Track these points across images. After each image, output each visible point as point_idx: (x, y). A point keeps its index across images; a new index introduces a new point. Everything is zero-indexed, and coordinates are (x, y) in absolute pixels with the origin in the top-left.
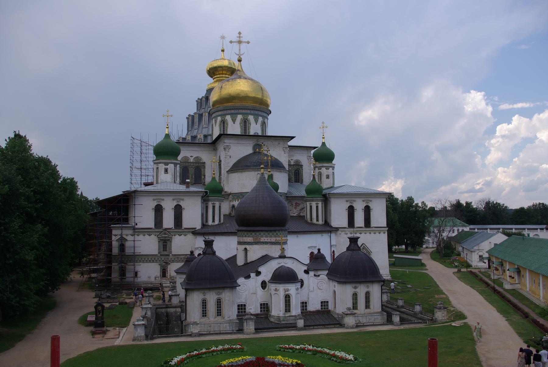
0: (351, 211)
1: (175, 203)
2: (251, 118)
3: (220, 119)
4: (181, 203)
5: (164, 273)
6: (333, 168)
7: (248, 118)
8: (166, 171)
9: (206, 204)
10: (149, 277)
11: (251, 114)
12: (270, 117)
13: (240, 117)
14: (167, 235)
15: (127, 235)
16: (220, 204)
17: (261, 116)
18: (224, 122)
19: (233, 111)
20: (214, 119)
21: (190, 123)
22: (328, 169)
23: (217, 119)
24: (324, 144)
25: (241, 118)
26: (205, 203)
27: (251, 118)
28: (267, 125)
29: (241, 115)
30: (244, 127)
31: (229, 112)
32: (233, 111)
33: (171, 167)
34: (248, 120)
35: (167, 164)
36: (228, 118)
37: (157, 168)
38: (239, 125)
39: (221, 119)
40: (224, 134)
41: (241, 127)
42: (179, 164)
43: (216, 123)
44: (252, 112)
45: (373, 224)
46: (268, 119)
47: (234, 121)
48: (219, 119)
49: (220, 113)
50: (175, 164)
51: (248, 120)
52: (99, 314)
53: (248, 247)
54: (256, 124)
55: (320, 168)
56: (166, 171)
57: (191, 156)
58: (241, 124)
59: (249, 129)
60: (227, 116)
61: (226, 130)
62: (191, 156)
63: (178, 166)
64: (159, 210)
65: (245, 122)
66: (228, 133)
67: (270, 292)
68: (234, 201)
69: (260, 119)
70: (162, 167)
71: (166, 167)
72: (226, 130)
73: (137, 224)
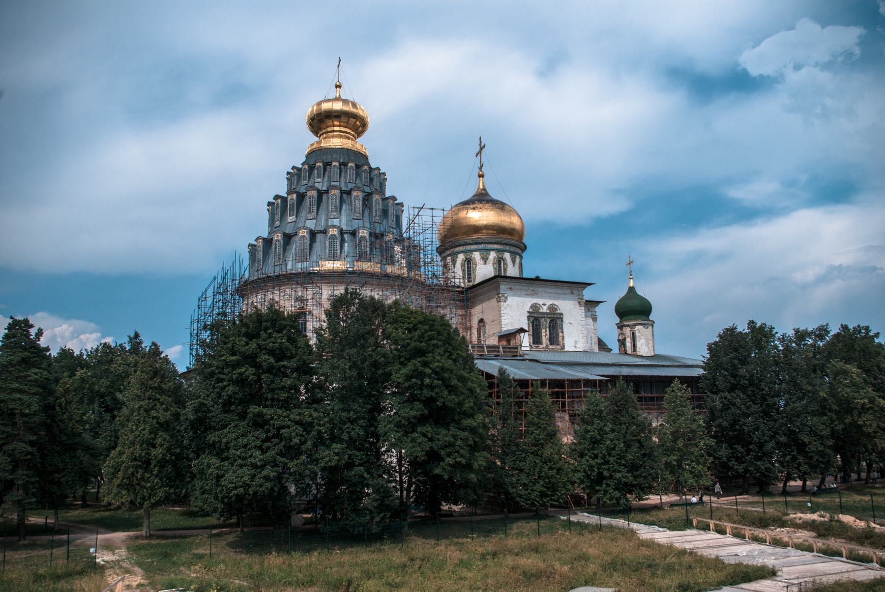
2: (507, 256)
11: (507, 251)
13: (493, 255)
20: (449, 259)
23: (457, 257)
34: (503, 260)
36: (477, 256)
40: (500, 276)
49: (461, 248)
51: (503, 260)
54: (514, 266)
60: (474, 253)
61: (473, 273)
65: (499, 262)
72: (473, 273)
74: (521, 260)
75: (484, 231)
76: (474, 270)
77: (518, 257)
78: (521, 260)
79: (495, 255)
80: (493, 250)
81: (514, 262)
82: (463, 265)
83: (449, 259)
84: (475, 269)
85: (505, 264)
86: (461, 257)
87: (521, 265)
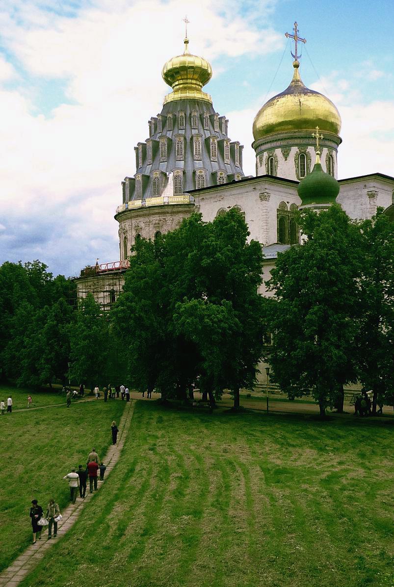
3: (267, 155)
7: (308, 150)
12: (340, 148)
13: (294, 150)
18: (272, 159)
21: (140, 155)
28: (335, 159)
30: (301, 165)
31: (278, 143)
34: (306, 155)
36: (278, 152)
38: (294, 162)
39: (269, 155)
40: (272, 177)
41: (297, 164)
46: (337, 152)
47: (286, 155)
65: (302, 157)
66: (278, 176)
75: (277, 129)
76: (275, 167)
79: (298, 150)
84: (276, 167)
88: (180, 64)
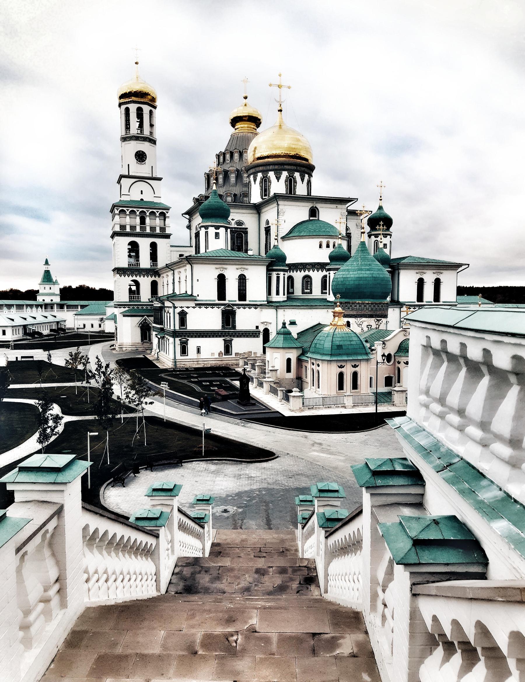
0: (421, 283)
1: (239, 272)
2: (297, 175)
4: (245, 273)
5: (228, 349)
6: (391, 235)
7: (295, 175)
8: (217, 235)
9: (269, 274)
10: (213, 354)
13: (285, 174)
14: (231, 308)
15: (188, 307)
16: (284, 274)
17: (307, 173)
18: (266, 179)
19: (278, 166)
20: (252, 176)
22: (386, 237)
24: (380, 208)
25: (287, 176)
26: (269, 273)
27: (297, 175)
29: (287, 172)
31: (271, 167)
32: (276, 167)
33: (222, 231)
34: (294, 179)
35: (217, 228)
36: (271, 175)
37: (207, 233)
41: (286, 185)
42: (229, 228)
43: (255, 180)
44: (299, 168)
45: (444, 297)
47: (278, 178)
48: (260, 175)
49: (261, 168)
50: (226, 228)
51: (294, 179)
52: (245, 387)
53: (350, 320)
55: (376, 236)
56: (217, 235)
57: (233, 220)
58: (287, 183)
59: (294, 189)
60: (270, 172)
62: (233, 220)
63: (229, 230)
64: (221, 280)
65: (291, 180)
67: (397, 365)
68: (291, 272)
69: (307, 176)
70: (212, 231)
71: (217, 231)
73: (198, 295)
74: (310, 178)
77: (307, 176)
78: (310, 178)
79: (288, 175)
80: (285, 170)
81: (303, 180)
82: (261, 182)
83: (252, 176)
85: (295, 182)
86: (260, 175)
87: (309, 182)
88: (128, 89)
